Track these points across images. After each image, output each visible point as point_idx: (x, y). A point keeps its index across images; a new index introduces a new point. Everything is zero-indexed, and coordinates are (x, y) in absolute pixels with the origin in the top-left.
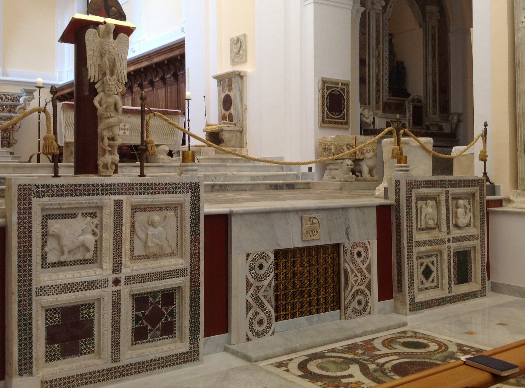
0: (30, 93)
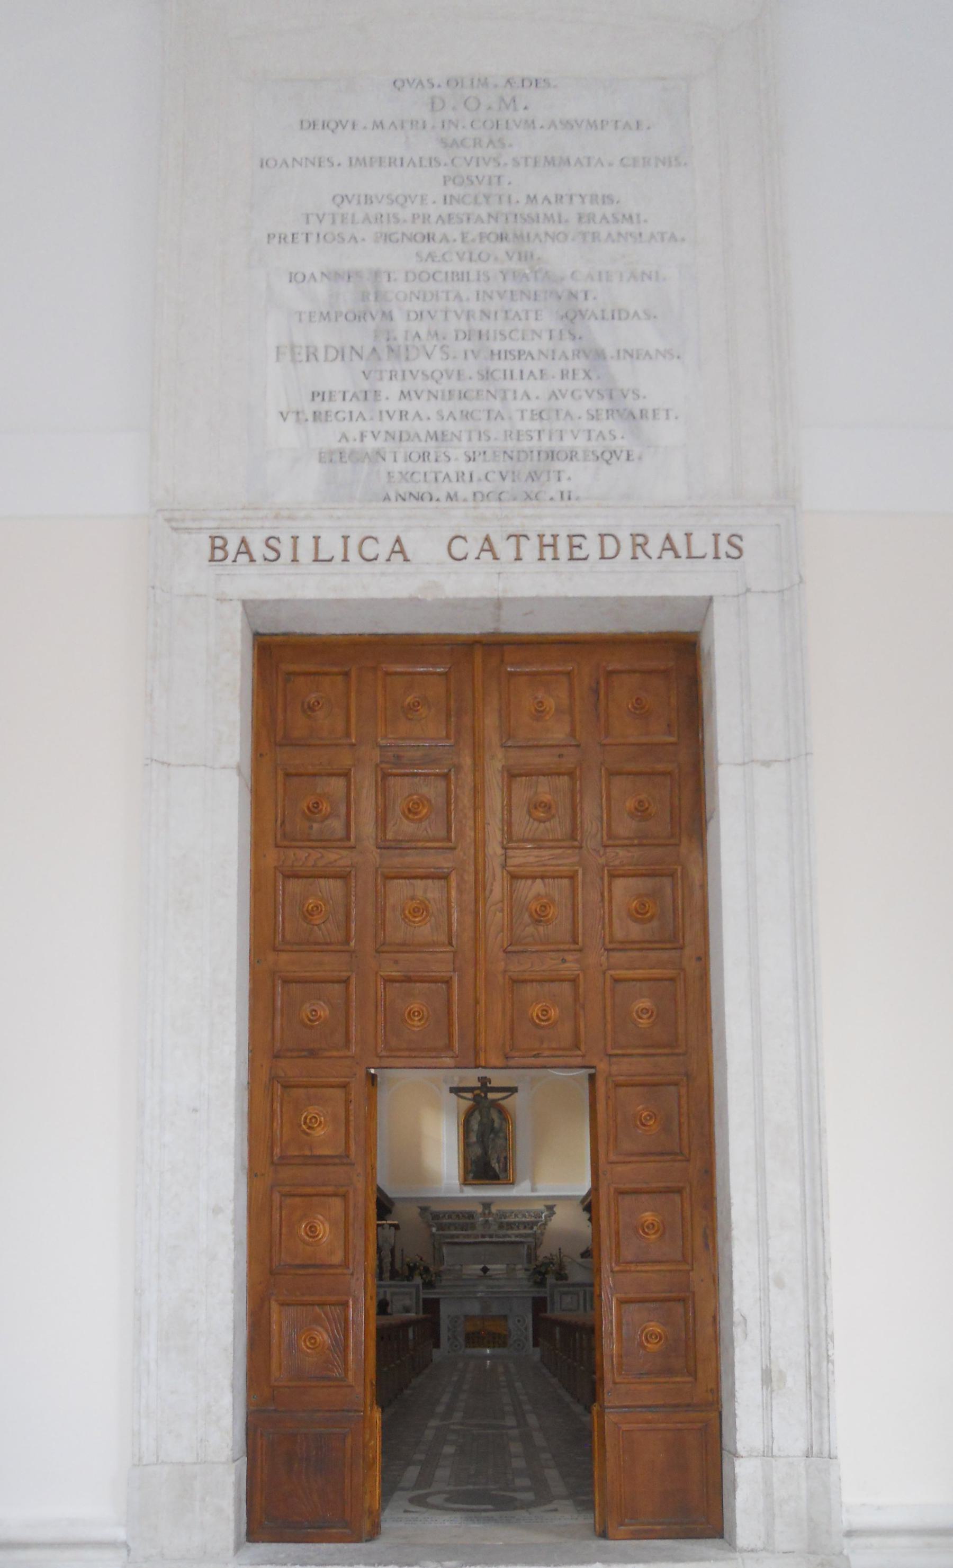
0: (550, 1209)
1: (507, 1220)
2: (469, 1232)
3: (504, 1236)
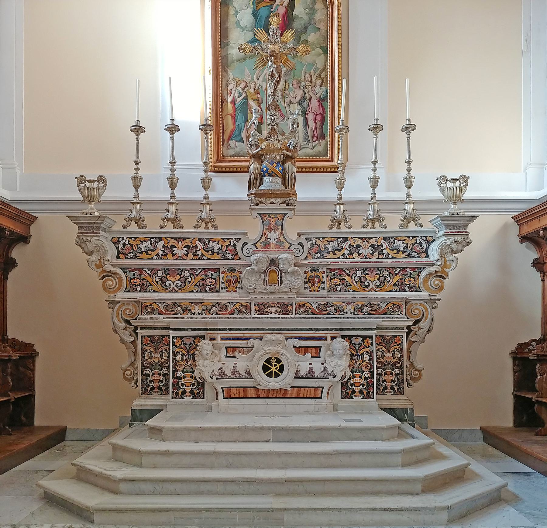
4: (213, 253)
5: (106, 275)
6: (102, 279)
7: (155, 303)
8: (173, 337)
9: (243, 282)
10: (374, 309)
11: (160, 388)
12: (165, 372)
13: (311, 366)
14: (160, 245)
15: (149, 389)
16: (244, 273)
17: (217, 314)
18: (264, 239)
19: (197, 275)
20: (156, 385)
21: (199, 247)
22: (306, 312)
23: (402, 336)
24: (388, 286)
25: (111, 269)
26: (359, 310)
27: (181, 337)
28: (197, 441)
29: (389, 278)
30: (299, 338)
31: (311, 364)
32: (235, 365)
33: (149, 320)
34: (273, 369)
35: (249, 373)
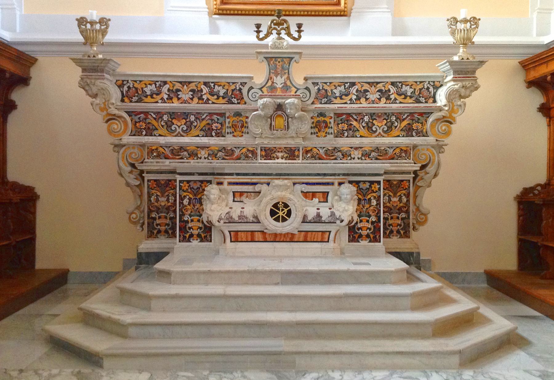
0: (466, 72)
1: (336, 106)
2: (229, 141)
3: (331, 154)
4: (218, 98)
5: (111, 118)
6: (107, 122)
7: (161, 147)
8: (180, 182)
9: (250, 127)
10: (380, 153)
11: (166, 232)
12: (172, 216)
13: (318, 211)
14: (165, 89)
15: (155, 232)
16: (250, 118)
17: (224, 159)
18: (270, 83)
19: (203, 120)
20: (163, 228)
21: (204, 92)
22: (313, 157)
23: (409, 181)
24: (395, 132)
25: (116, 112)
26: (366, 155)
27: (188, 182)
28: (207, 284)
29: (396, 124)
30: (307, 184)
31: (318, 209)
32: (242, 210)
33: (155, 164)
34: (281, 213)
35: (256, 217)
